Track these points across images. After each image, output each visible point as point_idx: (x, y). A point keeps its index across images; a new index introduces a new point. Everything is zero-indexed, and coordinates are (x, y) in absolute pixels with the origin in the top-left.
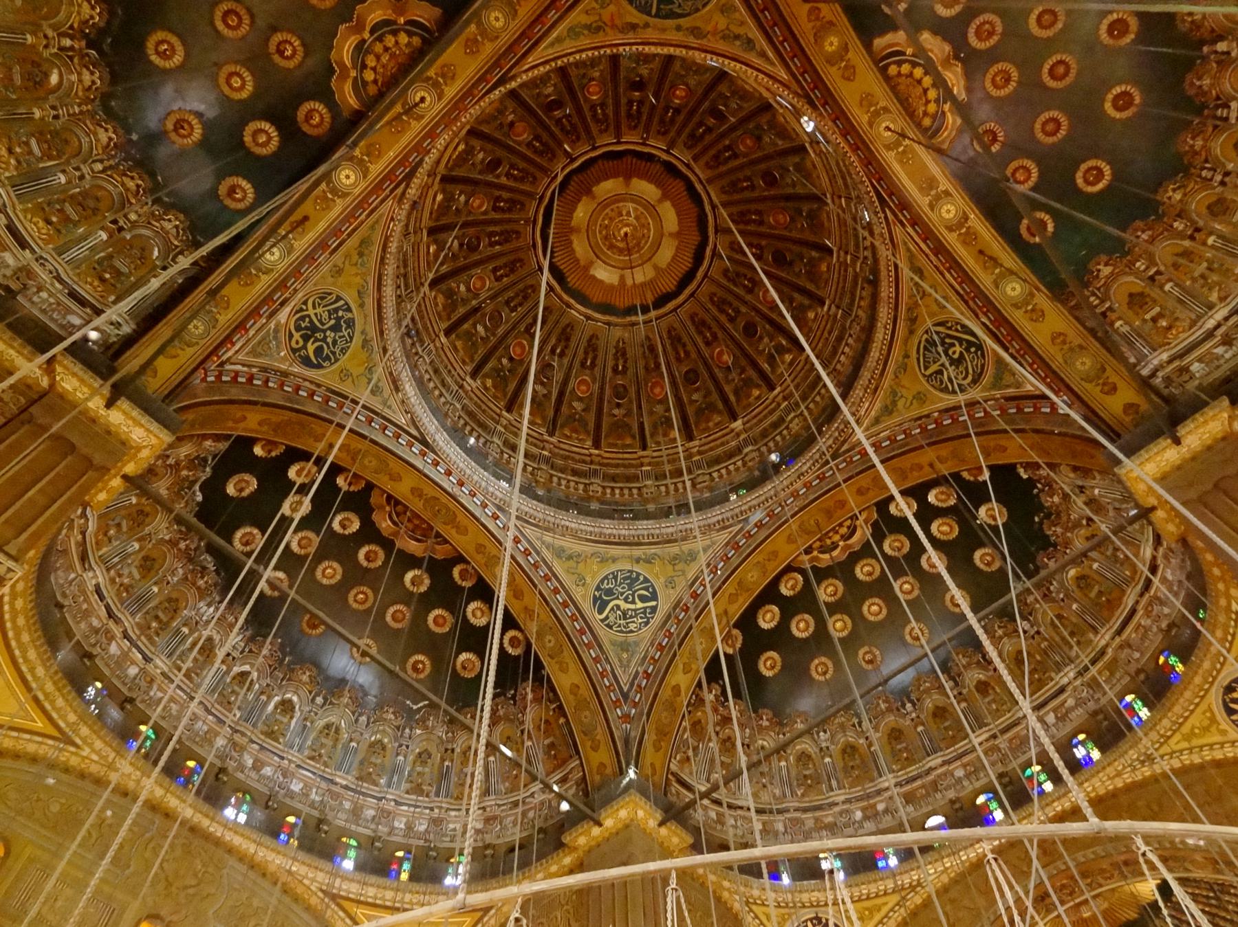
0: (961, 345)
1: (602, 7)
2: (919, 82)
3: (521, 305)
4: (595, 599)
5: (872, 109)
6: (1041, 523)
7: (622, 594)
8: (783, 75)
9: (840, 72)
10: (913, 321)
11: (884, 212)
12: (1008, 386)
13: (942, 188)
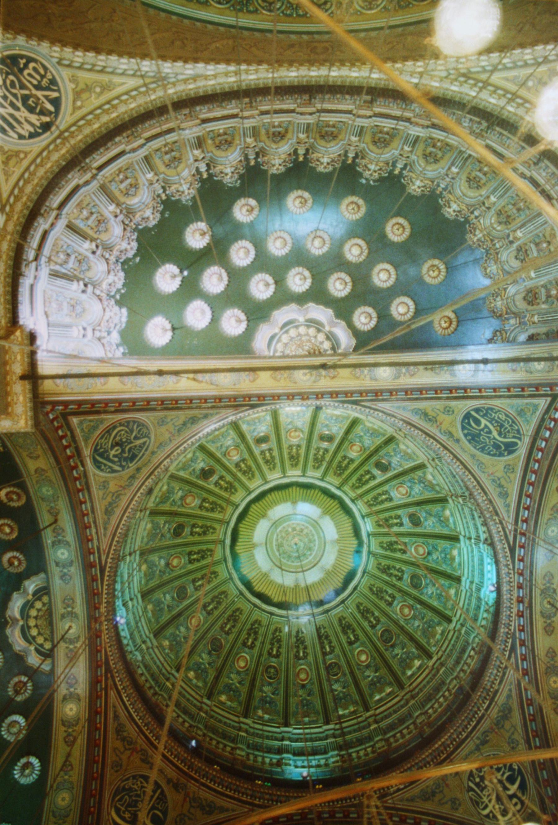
0: (108, 456)
1: (185, 815)
2: (36, 626)
3: (394, 567)
4: (510, 453)
5: (71, 647)
6: (135, 256)
7: (489, 437)
8: (112, 694)
9: (76, 686)
10: (133, 477)
11: (106, 562)
12: (91, 421)
13: (58, 569)
